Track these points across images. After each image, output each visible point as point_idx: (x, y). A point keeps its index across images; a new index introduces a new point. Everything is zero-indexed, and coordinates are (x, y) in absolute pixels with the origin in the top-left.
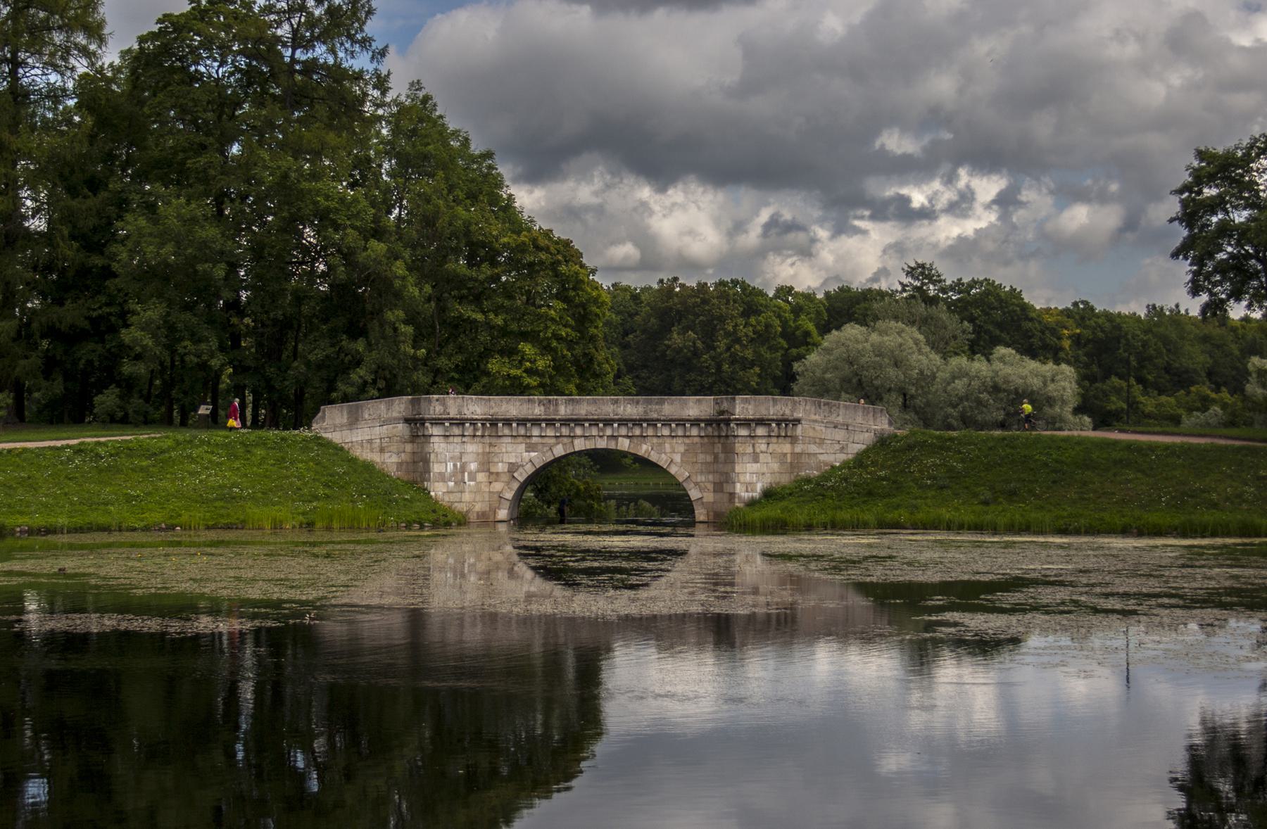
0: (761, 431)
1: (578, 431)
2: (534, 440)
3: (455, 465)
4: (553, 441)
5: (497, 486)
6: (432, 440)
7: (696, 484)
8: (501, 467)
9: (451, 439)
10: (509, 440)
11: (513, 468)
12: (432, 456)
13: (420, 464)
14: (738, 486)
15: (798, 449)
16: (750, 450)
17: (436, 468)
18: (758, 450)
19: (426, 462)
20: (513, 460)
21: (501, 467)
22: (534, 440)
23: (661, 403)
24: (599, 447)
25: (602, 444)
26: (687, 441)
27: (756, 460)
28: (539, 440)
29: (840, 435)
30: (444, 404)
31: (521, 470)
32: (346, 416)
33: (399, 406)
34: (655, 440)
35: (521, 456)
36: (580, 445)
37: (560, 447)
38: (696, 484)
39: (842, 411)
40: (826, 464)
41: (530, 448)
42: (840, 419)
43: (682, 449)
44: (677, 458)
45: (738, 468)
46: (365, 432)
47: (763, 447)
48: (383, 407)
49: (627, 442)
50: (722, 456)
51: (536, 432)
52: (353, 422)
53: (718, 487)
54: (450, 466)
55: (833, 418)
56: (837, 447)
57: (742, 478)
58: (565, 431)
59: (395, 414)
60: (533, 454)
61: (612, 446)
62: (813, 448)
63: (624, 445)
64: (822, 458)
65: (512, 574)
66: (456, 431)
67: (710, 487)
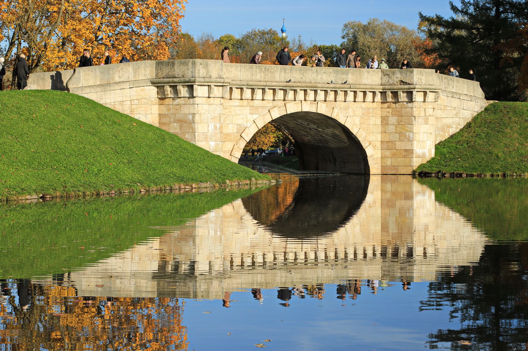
3: (215, 127)
4: (271, 104)
8: (231, 129)
10: (238, 103)
12: (197, 118)
14: (415, 143)
16: (422, 114)
17: (200, 128)
18: (427, 114)
20: (241, 123)
21: (231, 129)
23: (347, 73)
24: (305, 110)
27: (426, 123)
29: (455, 102)
30: (206, 66)
31: (247, 130)
32: (99, 79)
36: (293, 108)
37: (276, 109)
40: (449, 127)
41: (254, 110)
43: (359, 112)
44: (357, 120)
45: (415, 129)
47: (430, 112)
50: (393, 120)
52: (105, 86)
53: (387, 145)
55: (450, 89)
56: (454, 112)
57: (417, 137)
59: (142, 77)
60: (255, 116)
63: (323, 109)
66: (217, 92)
67: (379, 145)
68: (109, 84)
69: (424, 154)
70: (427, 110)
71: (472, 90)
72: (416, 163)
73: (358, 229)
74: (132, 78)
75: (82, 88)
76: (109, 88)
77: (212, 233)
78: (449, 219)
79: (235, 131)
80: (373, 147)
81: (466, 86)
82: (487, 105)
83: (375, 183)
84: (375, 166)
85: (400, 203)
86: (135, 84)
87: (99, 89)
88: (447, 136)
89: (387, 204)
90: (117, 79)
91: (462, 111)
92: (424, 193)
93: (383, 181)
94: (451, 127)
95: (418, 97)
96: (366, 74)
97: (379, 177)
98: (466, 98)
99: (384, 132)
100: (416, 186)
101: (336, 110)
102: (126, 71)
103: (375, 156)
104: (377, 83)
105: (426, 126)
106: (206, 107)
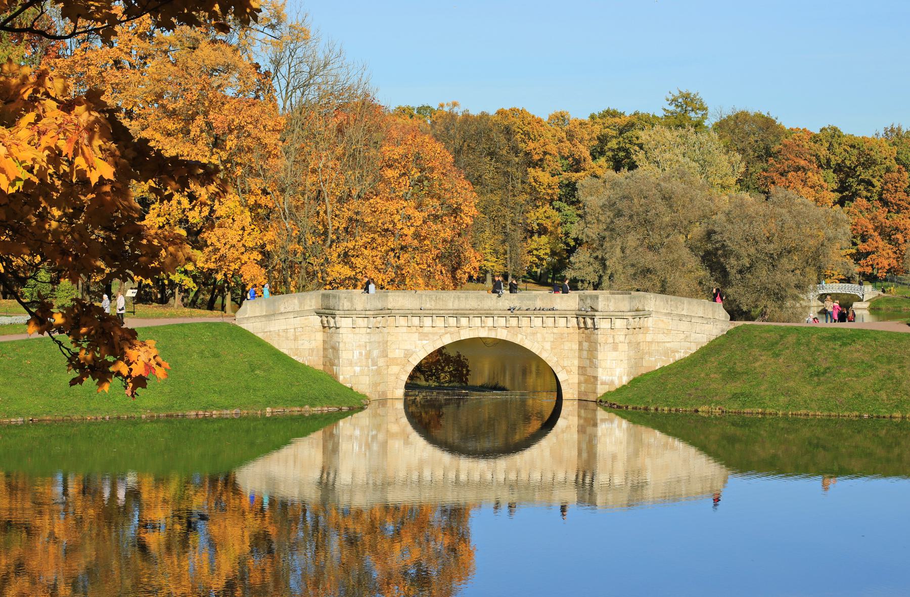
0: (619, 323)
1: (464, 321)
2: (426, 330)
3: (361, 354)
5: (394, 369)
6: (341, 330)
7: (564, 368)
9: (357, 330)
11: (408, 354)
12: (341, 345)
13: (331, 350)
14: (600, 370)
15: (649, 338)
17: (344, 355)
18: (617, 341)
19: (335, 349)
20: (408, 347)
22: (426, 330)
25: (483, 334)
26: (555, 330)
27: (615, 349)
28: (431, 329)
29: (684, 326)
31: (414, 356)
33: (312, 300)
34: (529, 330)
35: (416, 342)
36: (465, 335)
38: (564, 368)
39: (686, 306)
40: (674, 351)
41: (423, 336)
42: (684, 313)
43: (550, 337)
44: (548, 346)
46: (285, 325)
47: (622, 338)
48: (296, 301)
49: (505, 331)
50: (586, 345)
51: (427, 321)
52: (269, 316)
53: (582, 369)
54: (356, 353)
55: (679, 312)
56: (682, 336)
57: (603, 364)
58: (453, 321)
59: (307, 308)
60: (425, 342)
61: (492, 335)
62: (661, 338)
63: (502, 335)
64: (668, 345)
65: (407, 442)
66: (361, 322)
68: (273, 315)
69: (612, 382)
70: (616, 337)
71: (711, 312)
72: (601, 390)
73: (547, 453)
74: (297, 309)
75: (248, 318)
76: (273, 318)
77: (356, 448)
78: (673, 448)
79: (402, 355)
80: (567, 371)
81: (702, 308)
82: (732, 327)
83: (569, 409)
84: (569, 392)
85: (589, 430)
86: (299, 314)
87: (263, 319)
88: (672, 361)
89: (582, 430)
90: (282, 310)
91: (693, 335)
92: (612, 421)
93: (579, 406)
94: (678, 352)
95: (603, 325)
96: (558, 300)
97: (576, 403)
98: (700, 321)
99: (580, 357)
100: (601, 414)
101: (520, 336)
102: (290, 302)
103: (570, 382)
104: (573, 308)
105: (615, 354)
106: (351, 336)
